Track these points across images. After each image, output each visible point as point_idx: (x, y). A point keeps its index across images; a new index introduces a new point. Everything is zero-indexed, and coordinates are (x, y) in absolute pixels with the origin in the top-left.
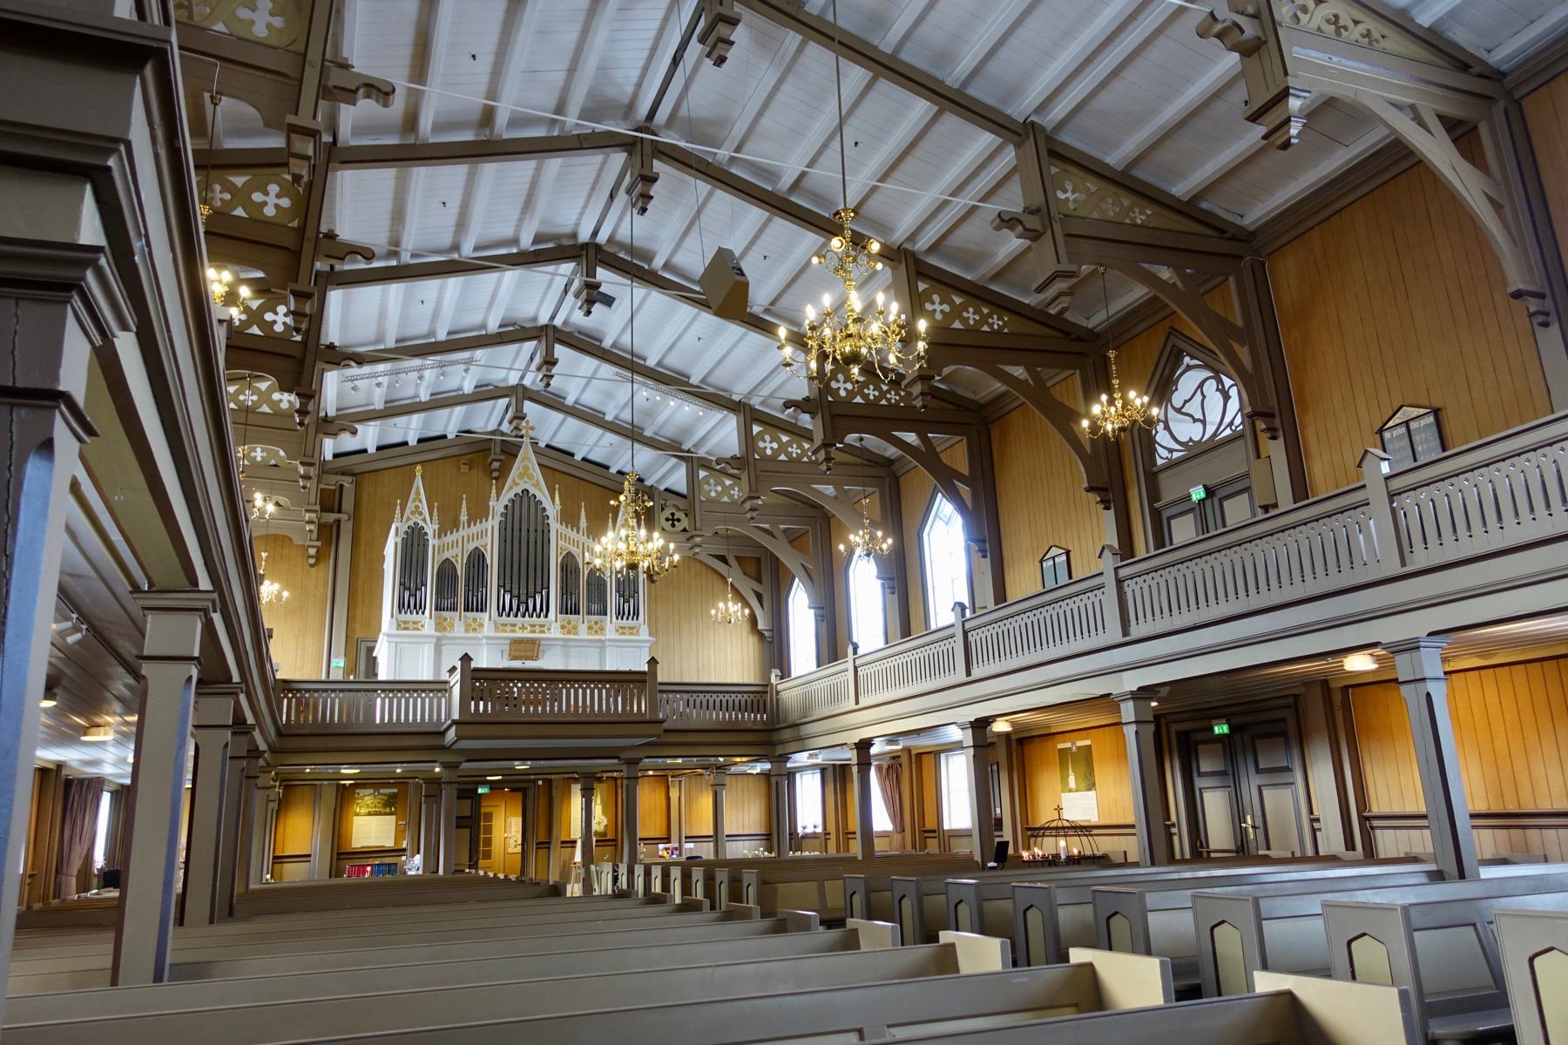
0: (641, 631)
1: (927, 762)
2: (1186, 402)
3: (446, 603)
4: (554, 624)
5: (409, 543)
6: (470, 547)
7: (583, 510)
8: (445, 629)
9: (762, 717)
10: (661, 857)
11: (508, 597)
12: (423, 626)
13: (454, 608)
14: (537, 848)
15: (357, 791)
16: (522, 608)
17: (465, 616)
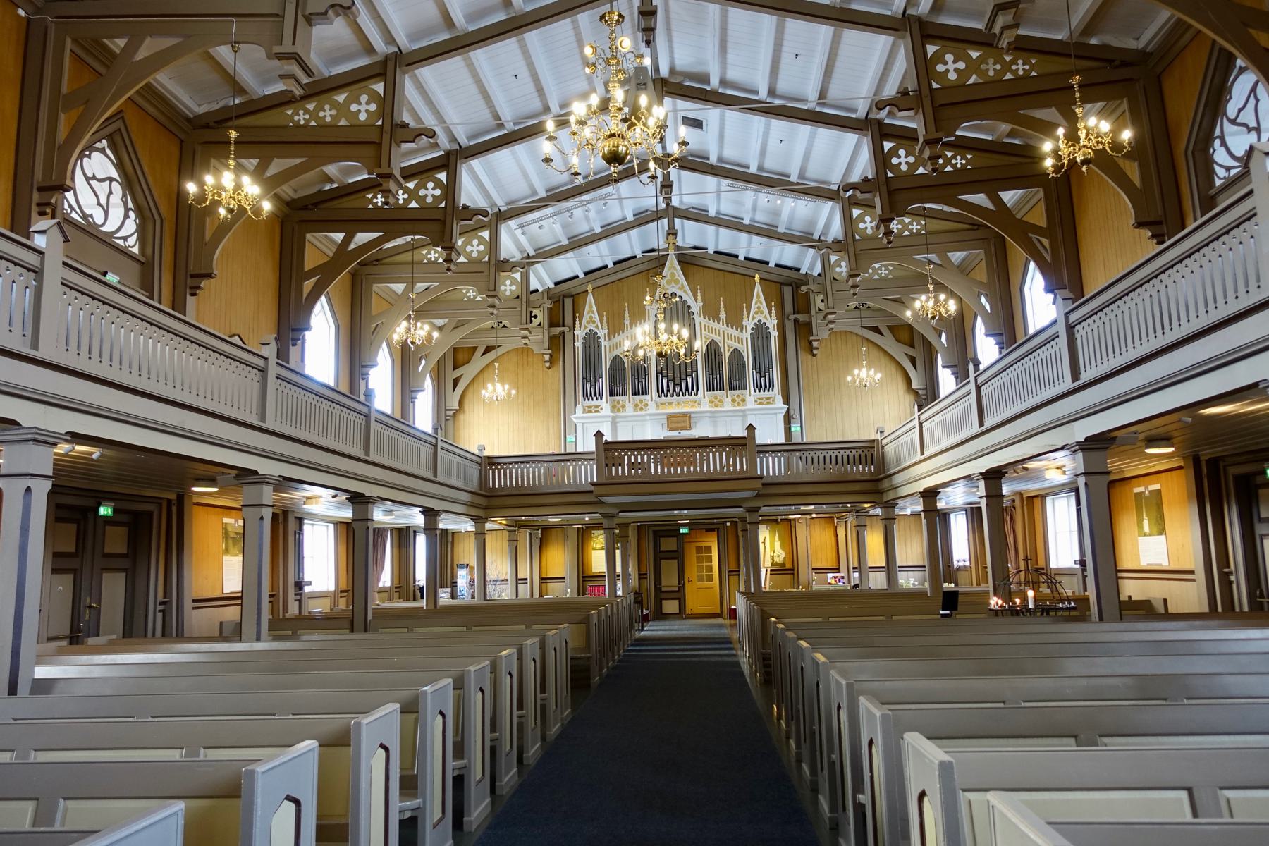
0: (776, 400)
1: (1037, 502)
2: (1240, 110)
3: (620, 389)
4: (703, 400)
5: (587, 346)
8: (619, 410)
9: (870, 469)
10: (830, 584)
11: (665, 381)
12: (602, 409)
13: (624, 394)
14: (729, 575)
15: (593, 532)
16: (677, 389)
17: (633, 399)
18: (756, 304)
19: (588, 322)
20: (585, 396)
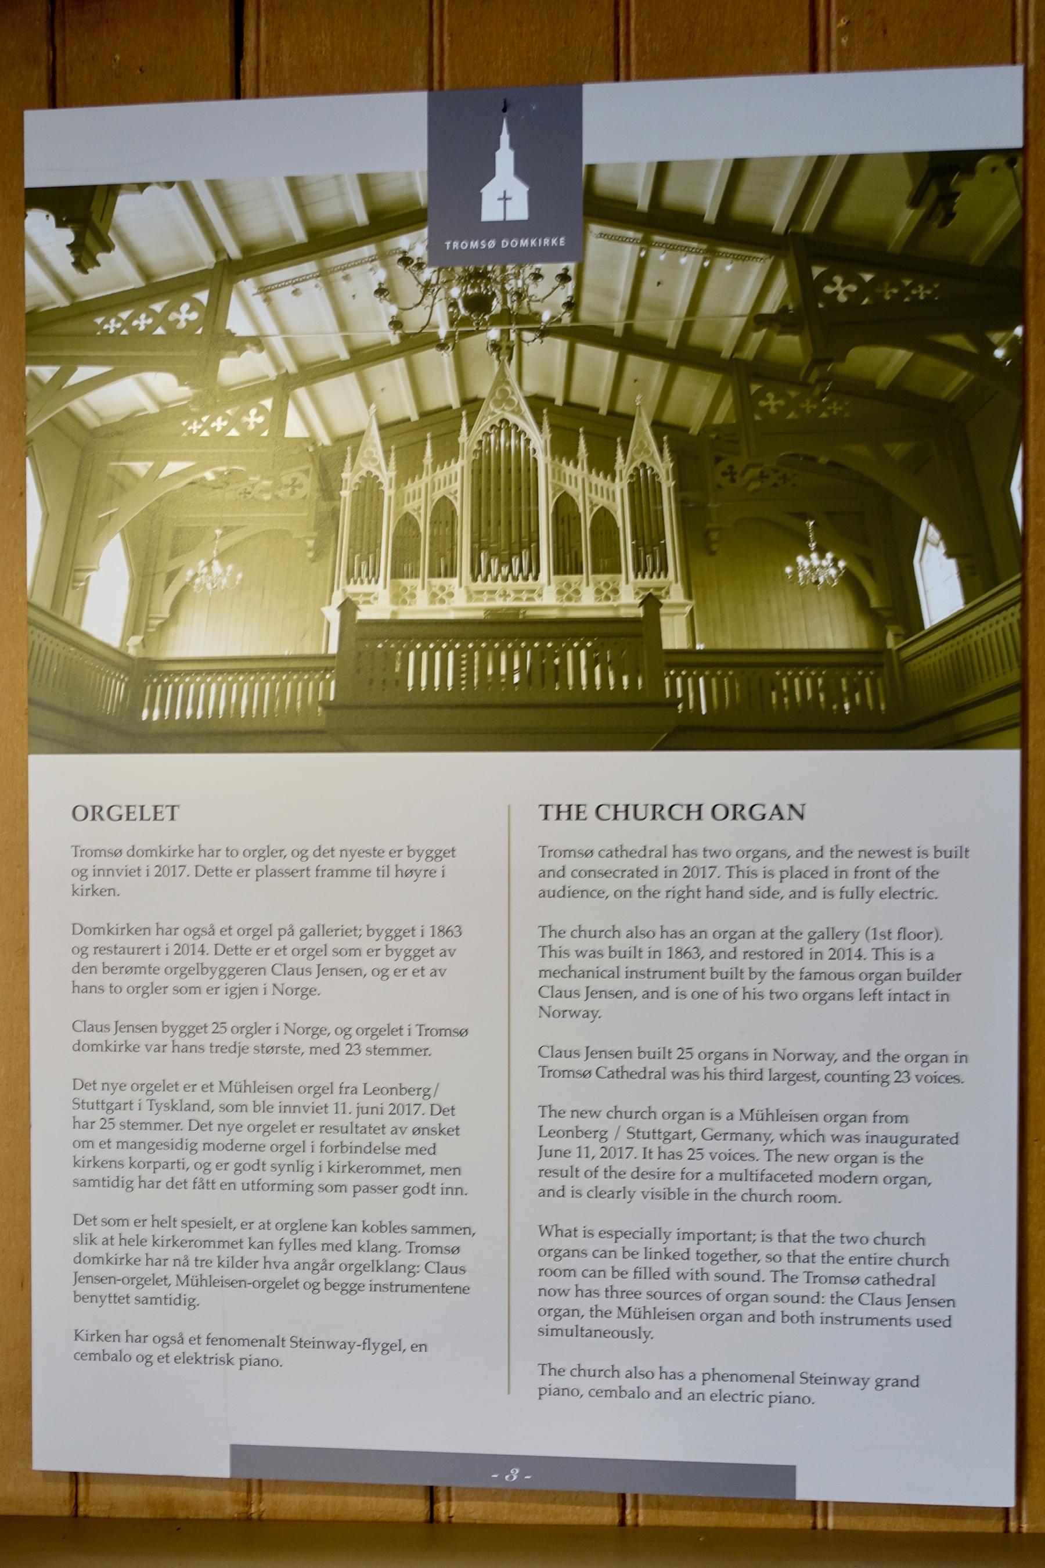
3: (408, 567)
4: (546, 589)
8: (404, 602)
20: (349, 575)
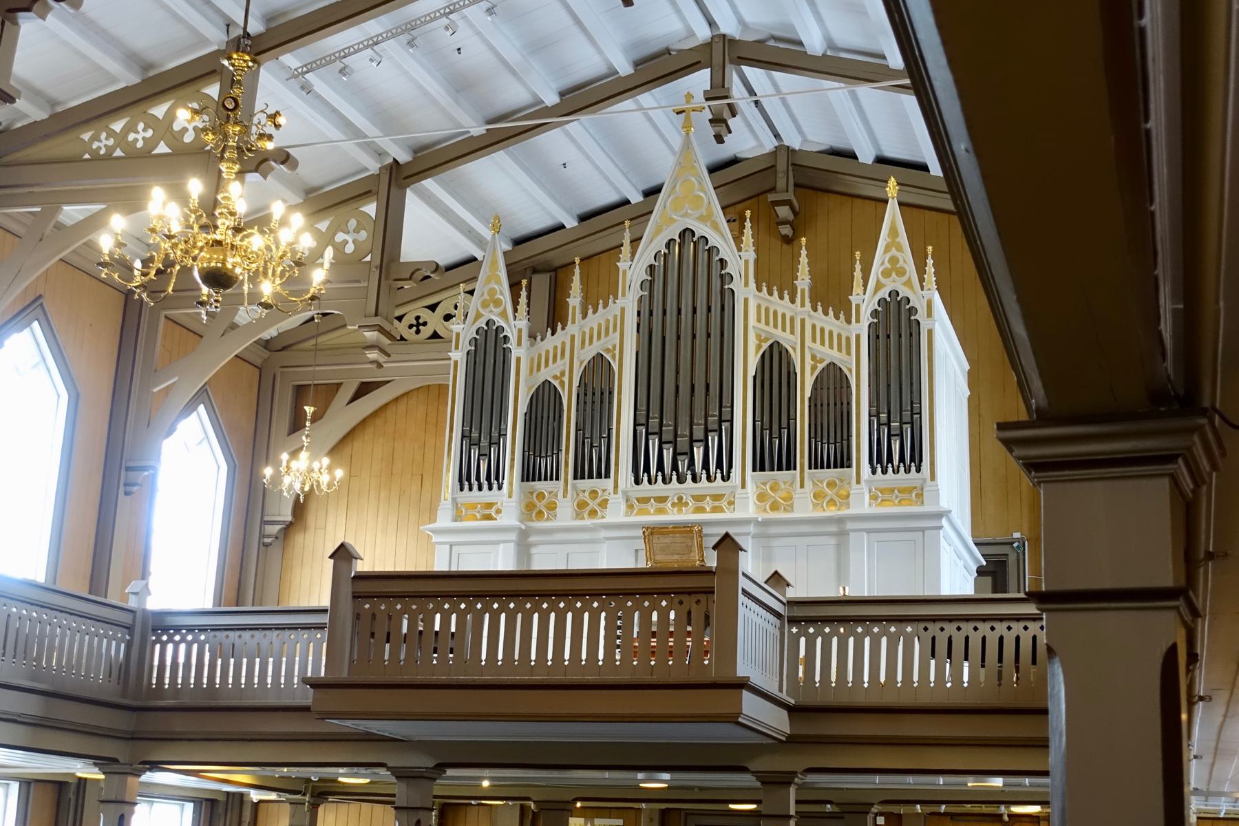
3: (544, 464)
6: (588, 353)
7: (804, 252)
11: (654, 443)
16: (683, 464)
17: (574, 486)
18: (887, 249)
19: (485, 305)
